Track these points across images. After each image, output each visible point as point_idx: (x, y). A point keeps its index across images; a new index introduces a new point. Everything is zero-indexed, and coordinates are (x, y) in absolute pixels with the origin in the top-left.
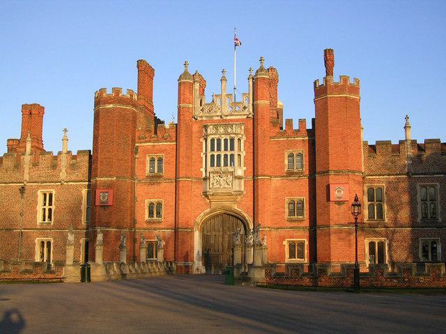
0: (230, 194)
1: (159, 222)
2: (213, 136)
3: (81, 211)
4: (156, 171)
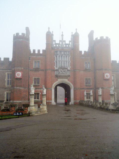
0: (65, 76)
1: (39, 86)
2: (59, 55)
3: (5, 81)
4: (37, 67)
